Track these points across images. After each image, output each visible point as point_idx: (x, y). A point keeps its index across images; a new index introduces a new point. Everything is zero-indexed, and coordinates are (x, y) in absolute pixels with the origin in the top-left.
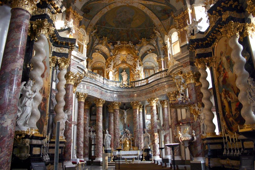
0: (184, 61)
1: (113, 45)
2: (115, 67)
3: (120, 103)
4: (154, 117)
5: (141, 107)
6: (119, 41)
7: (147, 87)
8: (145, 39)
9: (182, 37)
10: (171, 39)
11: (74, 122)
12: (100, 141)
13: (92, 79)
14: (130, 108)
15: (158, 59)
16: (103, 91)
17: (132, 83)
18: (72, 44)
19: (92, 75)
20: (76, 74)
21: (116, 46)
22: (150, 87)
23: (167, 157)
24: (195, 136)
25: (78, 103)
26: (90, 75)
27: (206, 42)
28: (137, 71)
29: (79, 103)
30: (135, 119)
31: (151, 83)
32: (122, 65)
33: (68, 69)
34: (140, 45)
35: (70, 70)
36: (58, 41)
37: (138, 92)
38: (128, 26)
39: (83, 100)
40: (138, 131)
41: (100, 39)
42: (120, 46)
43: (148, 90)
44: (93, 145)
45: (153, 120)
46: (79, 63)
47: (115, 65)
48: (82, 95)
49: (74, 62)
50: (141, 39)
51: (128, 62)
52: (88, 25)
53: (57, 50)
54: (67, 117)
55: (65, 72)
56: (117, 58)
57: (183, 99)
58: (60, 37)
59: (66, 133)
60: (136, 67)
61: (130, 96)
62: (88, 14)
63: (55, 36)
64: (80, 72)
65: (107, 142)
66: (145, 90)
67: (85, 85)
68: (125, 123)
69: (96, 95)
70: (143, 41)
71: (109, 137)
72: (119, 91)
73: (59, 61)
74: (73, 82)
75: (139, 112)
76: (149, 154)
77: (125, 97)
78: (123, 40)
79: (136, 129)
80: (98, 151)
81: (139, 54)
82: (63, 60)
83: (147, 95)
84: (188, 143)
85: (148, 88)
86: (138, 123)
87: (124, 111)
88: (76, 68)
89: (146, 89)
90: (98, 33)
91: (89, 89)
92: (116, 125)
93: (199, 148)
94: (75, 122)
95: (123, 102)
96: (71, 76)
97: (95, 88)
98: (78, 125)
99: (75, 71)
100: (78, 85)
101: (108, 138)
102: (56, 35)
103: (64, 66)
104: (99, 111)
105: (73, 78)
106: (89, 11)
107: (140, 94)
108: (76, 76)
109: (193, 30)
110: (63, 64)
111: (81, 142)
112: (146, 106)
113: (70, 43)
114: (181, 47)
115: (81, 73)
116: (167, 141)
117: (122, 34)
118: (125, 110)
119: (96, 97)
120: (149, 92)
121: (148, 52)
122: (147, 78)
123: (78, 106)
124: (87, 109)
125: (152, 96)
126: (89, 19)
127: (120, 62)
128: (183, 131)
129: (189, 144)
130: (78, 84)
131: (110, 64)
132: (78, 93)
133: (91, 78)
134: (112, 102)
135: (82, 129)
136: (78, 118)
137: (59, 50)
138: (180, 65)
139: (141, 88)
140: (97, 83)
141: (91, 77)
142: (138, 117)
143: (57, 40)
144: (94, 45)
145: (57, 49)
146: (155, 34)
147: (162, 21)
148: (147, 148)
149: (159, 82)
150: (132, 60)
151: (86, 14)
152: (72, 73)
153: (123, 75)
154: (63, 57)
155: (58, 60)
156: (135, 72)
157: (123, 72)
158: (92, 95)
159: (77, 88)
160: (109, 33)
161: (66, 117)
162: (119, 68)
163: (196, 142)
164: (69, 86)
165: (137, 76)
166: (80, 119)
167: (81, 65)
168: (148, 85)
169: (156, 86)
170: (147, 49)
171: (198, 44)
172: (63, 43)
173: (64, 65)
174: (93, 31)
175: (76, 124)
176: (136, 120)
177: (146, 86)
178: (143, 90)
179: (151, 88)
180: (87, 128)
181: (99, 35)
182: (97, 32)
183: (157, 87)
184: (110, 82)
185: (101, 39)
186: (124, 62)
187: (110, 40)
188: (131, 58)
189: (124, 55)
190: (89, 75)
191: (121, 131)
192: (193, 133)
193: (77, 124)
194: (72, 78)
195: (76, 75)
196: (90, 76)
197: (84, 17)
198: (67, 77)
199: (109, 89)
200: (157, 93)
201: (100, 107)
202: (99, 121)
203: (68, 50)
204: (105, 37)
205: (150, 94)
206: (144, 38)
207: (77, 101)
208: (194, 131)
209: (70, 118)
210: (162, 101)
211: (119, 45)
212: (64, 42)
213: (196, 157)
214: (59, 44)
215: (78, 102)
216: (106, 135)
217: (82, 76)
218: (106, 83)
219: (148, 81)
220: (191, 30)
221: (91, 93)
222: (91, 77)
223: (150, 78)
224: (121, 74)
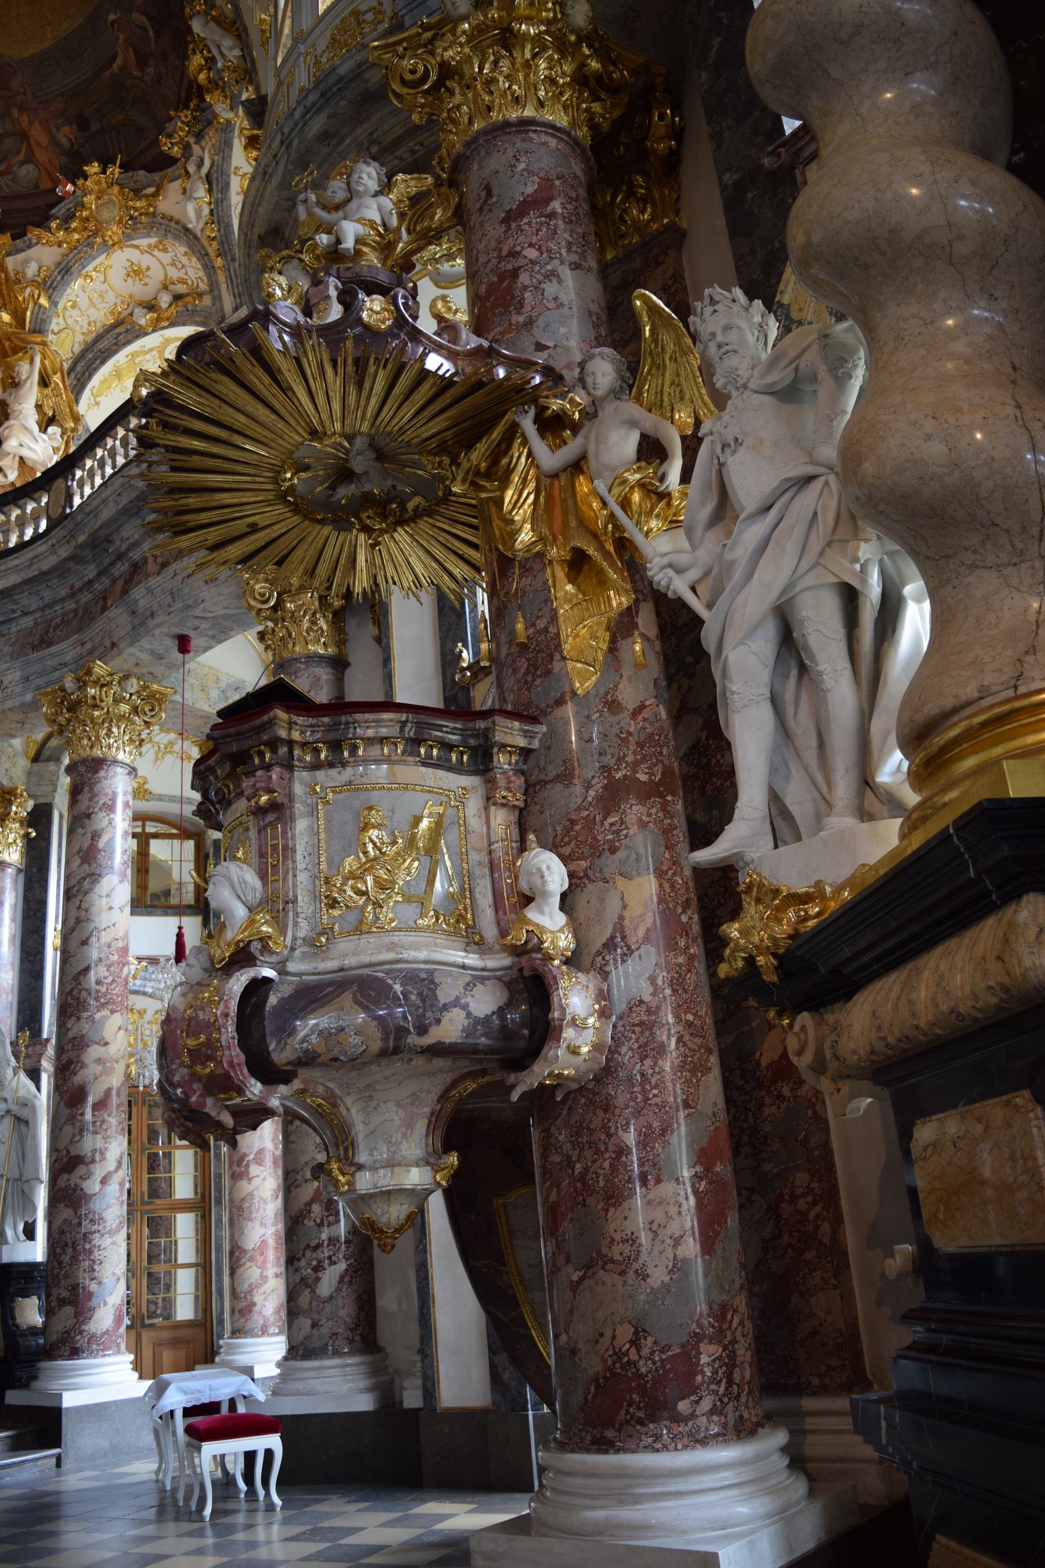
4: (95, 877)
7: (51, 561)
8: (115, 171)
22: (73, 558)
43: (63, 593)
45: (78, 921)
50: (76, 174)
66: (31, 602)
70: (98, 188)
83: (50, 644)
84: (421, 1126)
85: (60, 570)
89: (42, 577)
93: (667, 1222)
116: (254, 1170)
120: (75, 612)
121: (143, 319)
128: (335, 864)
129: (453, 1159)
169: (131, 531)
170: (140, 290)
177: (40, 548)
192: (527, 900)
208: (552, 872)
213: (603, 1446)
219: (70, 497)
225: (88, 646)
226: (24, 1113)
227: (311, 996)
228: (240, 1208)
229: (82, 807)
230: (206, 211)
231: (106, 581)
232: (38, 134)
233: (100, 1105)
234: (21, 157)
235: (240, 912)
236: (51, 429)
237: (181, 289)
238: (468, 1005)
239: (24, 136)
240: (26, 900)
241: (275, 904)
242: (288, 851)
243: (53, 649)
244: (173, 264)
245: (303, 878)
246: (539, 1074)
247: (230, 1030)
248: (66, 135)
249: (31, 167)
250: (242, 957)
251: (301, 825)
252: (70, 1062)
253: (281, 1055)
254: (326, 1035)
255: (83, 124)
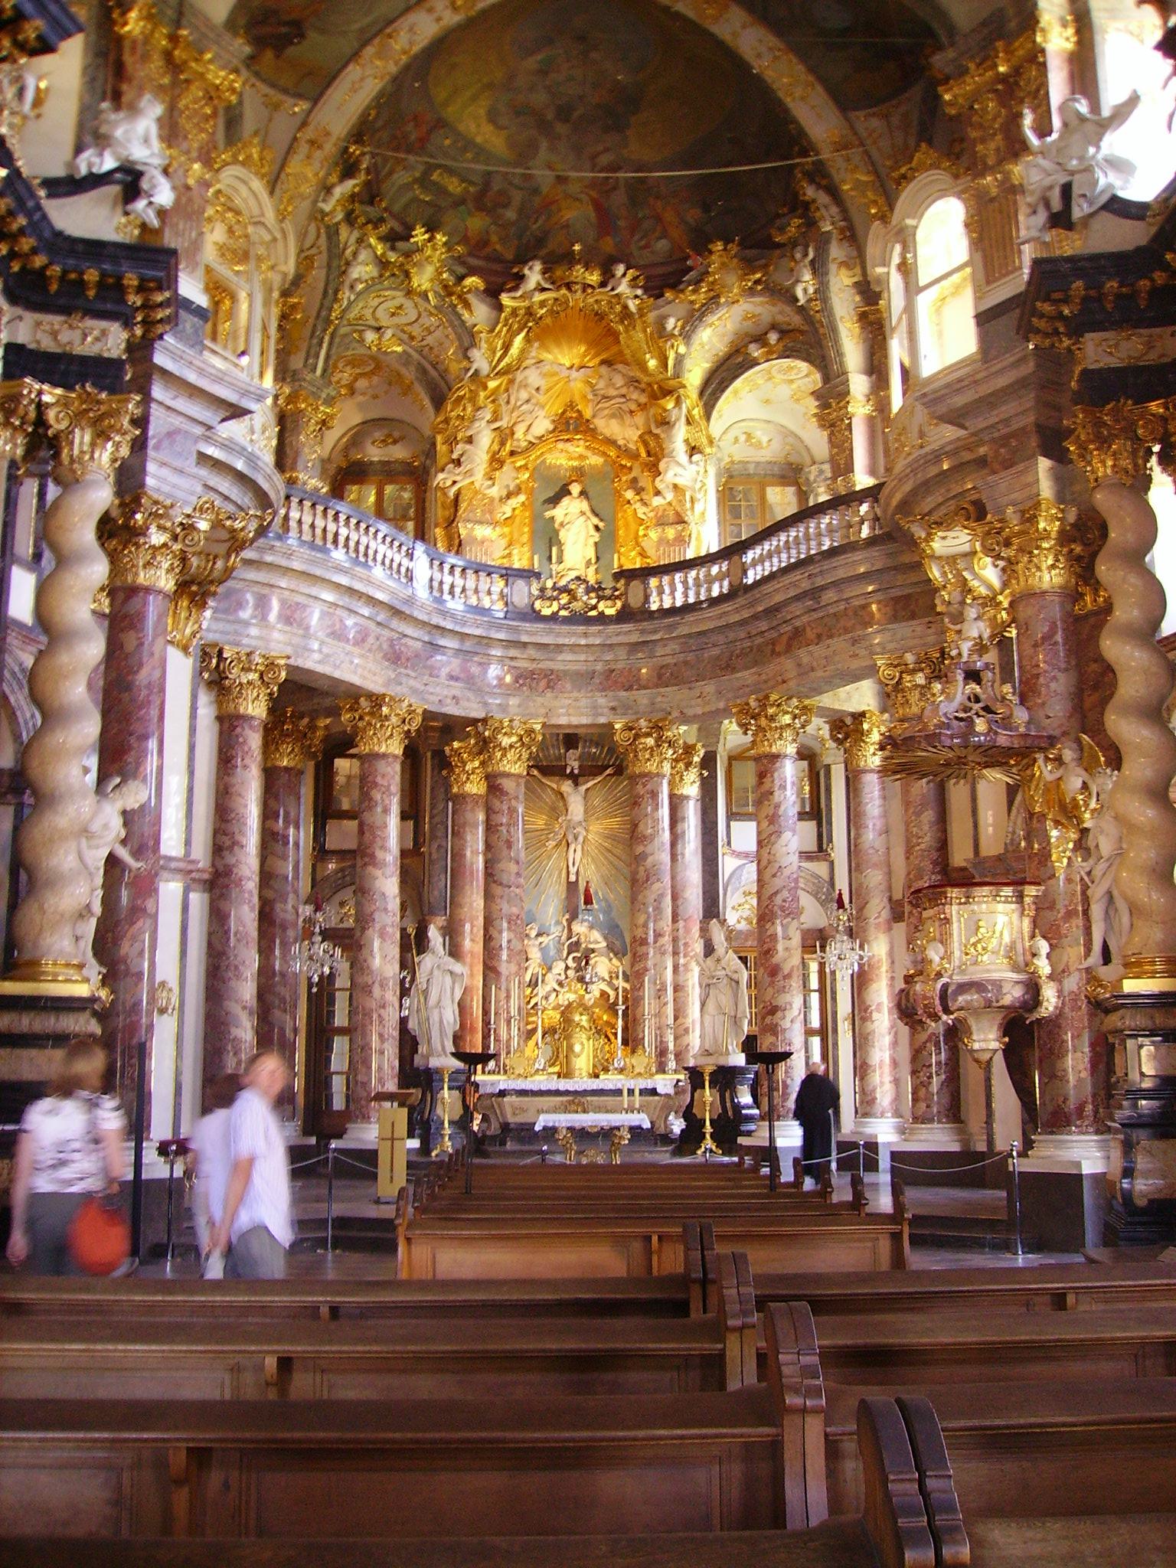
0: (992, 426)
1: (492, 293)
2: (502, 463)
3: (538, 727)
5: (688, 765)
6: (538, 266)
7: (736, 618)
8: (734, 248)
9: (989, 234)
10: (915, 256)
11: (182, 865)
12: (384, 1007)
13: (323, 550)
14: (608, 772)
15: (824, 405)
16: (410, 642)
17: (627, 585)
18: (151, 290)
19: (320, 523)
20: (188, 511)
21: (514, 304)
23: (868, 1130)
24: (1051, 977)
25: (216, 727)
26: (307, 519)
27: (1152, 280)
28: (670, 496)
29: (229, 724)
30: (639, 849)
31: (768, 588)
32: (560, 445)
33: (129, 481)
34: (694, 291)
35: (143, 485)
36: (45, 268)
37: (668, 650)
38: (607, 150)
39: (256, 708)
40: (658, 935)
41: (393, 248)
42: (542, 304)
44: (342, 1031)
45: (769, 862)
46: (210, 428)
47: (503, 444)
48: (249, 670)
49: (177, 421)
51: (600, 423)
52: (295, 139)
53: (39, 335)
54: (117, 822)
55: (99, 496)
56: (524, 395)
57: (977, 707)
58: (59, 234)
59: (116, 942)
60: (662, 466)
61: (608, 678)
62: (291, 51)
63: (22, 231)
64: (226, 498)
65: (436, 1012)
66: (720, 639)
67: (266, 591)
68: (573, 878)
69: (353, 667)
71: (448, 979)
72: (525, 639)
73: (51, 415)
74: (168, 571)
75: (671, 796)
76: (738, 1108)
77: (568, 686)
78: (569, 259)
79: (645, 925)
80: (365, 1079)
81: (688, 364)
82: (87, 411)
83: (734, 670)
84: (995, 1028)
85: (743, 623)
86: (667, 880)
87: (567, 787)
88: (190, 464)
90: (371, 203)
91: (300, 625)
92: (498, 890)
93: (1076, 1064)
94: (193, 862)
95: (554, 721)
96: (153, 529)
97: (344, 614)
98: (217, 883)
99: (180, 494)
100: (215, 594)
101: (443, 982)
102: (22, 221)
103: (92, 457)
104: (376, 784)
105: (165, 545)
106: (297, 30)
107: (686, 663)
108: (189, 528)
109: (1067, 190)
110: (82, 438)
111: (235, 1008)
112: (731, 759)
113: (131, 280)
114: (984, 319)
115: (231, 508)
116: (875, 1015)
117: (554, 208)
118: (576, 784)
119: (356, 680)
120: (751, 648)
121: (756, 352)
122: (732, 552)
123: (220, 750)
124: (286, 769)
125: (766, 682)
126: (300, 96)
127: (542, 425)
129: (1007, 1039)
130: (212, 582)
131: (470, 440)
132: (220, 652)
133: (312, 545)
134: (474, 722)
135: (245, 917)
136: (217, 832)
137: (54, 334)
138: (967, 456)
139: (690, 618)
140: (361, 579)
141: (319, 531)
142: (666, 836)
143: (39, 261)
144: (346, 295)
145: (38, 324)
146: (805, 209)
147: (853, 115)
148: (722, 1062)
149: (820, 582)
150: (633, 407)
151: (278, 57)
152: (156, 503)
153: (562, 525)
154: (83, 386)
155: (48, 405)
156: (657, 501)
157: (566, 501)
158: (320, 669)
159: (208, 613)
160: (459, 202)
161: (106, 826)
162: (540, 473)
163: (1054, 1024)
164: (135, 603)
165: (671, 533)
166: (228, 843)
167: (228, 446)
168: (741, 601)
169: (797, 608)
171: (1093, 293)
172: (81, 284)
173: (93, 445)
174: (333, 186)
175: (205, 881)
176: (650, 860)
177: (726, 607)
178: (700, 633)
179: (763, 625)
180: (290, 906)
181: (382, 220)
182: (370, 194)
183: (805, 619)
184: (458, 571)
185: (400, 245)
186: (571, 424)
187: (470, 254)
188: (624, 391)
189: (574, 374)
190: (300, 522)
191: (539, 935)
192: (1034, 955)
193: (206, 876)
194: (157, 538)
195: (188, 516)
196: (306, 527)
197: (264, 81)
198: (117, 532)
199: (449, 626)
200: (805, 660)
201: (384, 756)
202: (373, 856)
203: (125, 335)
204: (431, 229)
205: (756, 663)
206: (727, 241)
207: (206, 711)
208: (1043, 946)
209: (140, 830)
210: (848, 721)
211: (538, 297)
212: (92, 275)
213: (1052, 1133)
214: (54, 287)
215: (220, 719)
216: (426, 963)
217: (238, 525)
218: (431, 580)
219: (745, 573)
220: (1051, 188)
221: (316, 656)
222: (319, 531)
223: (758, 550)
224: (548, 514)
225: (764, 677)
226: (735, 976)
227: (963, 988)
228: (866, 1039)
229: (766, 786)
230: (811, 290)
231: (774, 634)
232: (669, 216)
233: (788, 976)
234: (657, 234)
235: (937, 959)
236: (696, 458)
237: (785, 327)
238: (1013, 994)
239: (659, 219)
240: (703, 821)
241: (947, 956)
242: (951, 935)
243: (739, 675)
244: (780, 313)
245: (956, 945)
246: (1036, 1016)
247: (937, 1002)
248: (693, 215)
249: (664, 242)
250: (939, 975)
251: (955, 925)
252: (768, 951)
253: (952, 1006)
254: (967, 1002)
255: (706, 208)
